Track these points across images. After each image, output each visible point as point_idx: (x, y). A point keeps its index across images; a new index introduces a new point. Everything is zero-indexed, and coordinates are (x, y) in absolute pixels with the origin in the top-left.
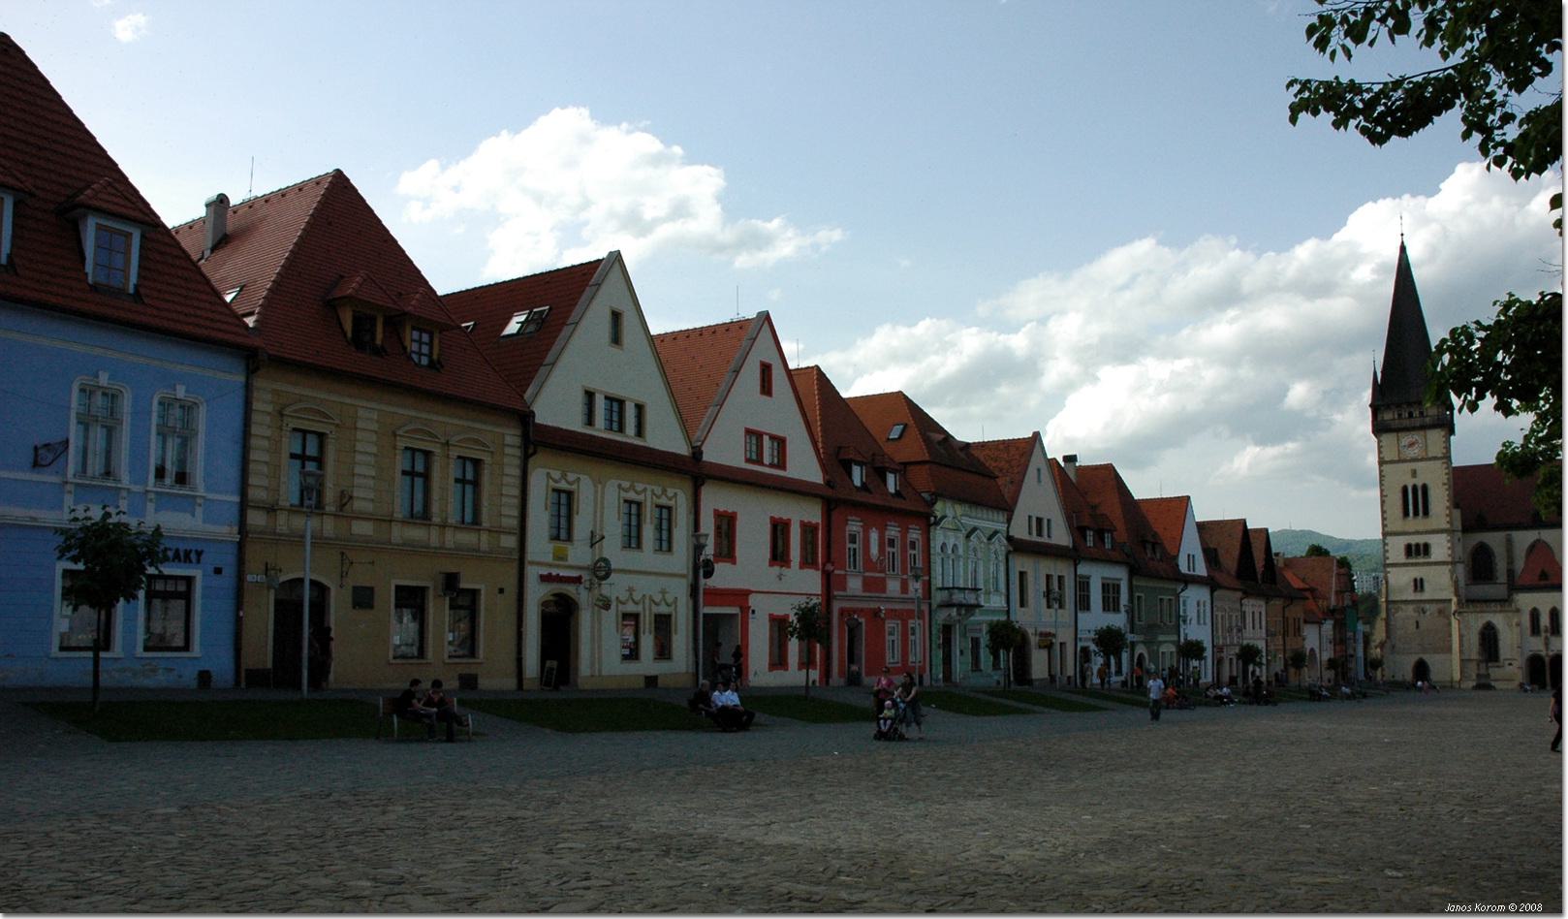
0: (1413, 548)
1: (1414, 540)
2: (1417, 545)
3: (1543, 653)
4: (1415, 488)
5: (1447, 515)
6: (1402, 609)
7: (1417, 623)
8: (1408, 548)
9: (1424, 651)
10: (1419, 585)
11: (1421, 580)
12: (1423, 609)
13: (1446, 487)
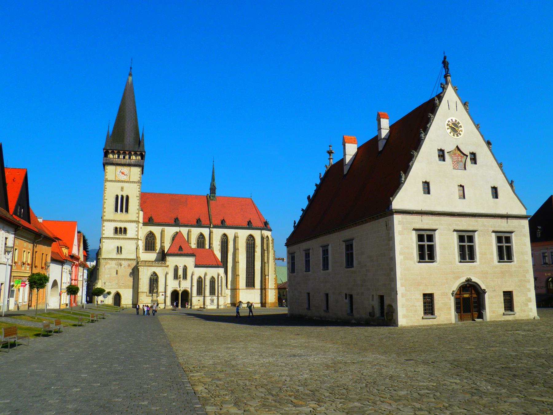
0: (118, 229)
1: (119, 225)
2: (121, 228)
3: (178, 289)
4: (122, 197)
5: (137, 213)
6: (109, 263)
7: (117, 271)
8: (116, 228)
9: (120, 287)
10: (119, 250)
11: (121, 247)
12: (120, 264)
13: (138, 198)
